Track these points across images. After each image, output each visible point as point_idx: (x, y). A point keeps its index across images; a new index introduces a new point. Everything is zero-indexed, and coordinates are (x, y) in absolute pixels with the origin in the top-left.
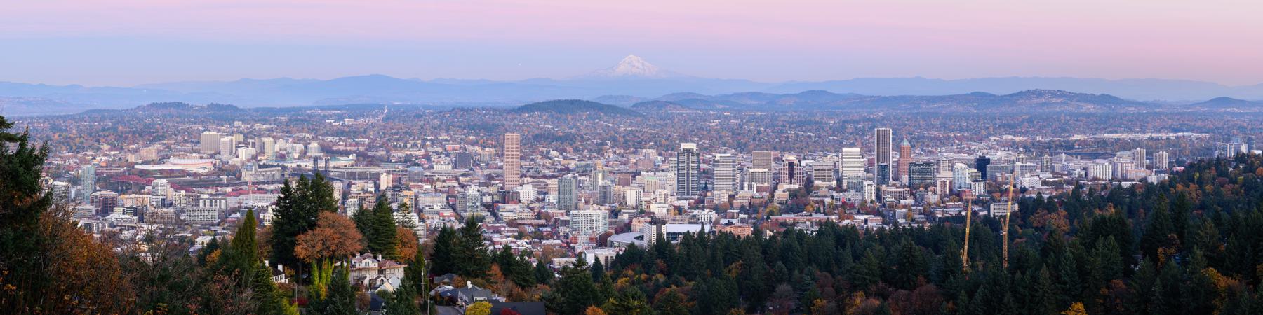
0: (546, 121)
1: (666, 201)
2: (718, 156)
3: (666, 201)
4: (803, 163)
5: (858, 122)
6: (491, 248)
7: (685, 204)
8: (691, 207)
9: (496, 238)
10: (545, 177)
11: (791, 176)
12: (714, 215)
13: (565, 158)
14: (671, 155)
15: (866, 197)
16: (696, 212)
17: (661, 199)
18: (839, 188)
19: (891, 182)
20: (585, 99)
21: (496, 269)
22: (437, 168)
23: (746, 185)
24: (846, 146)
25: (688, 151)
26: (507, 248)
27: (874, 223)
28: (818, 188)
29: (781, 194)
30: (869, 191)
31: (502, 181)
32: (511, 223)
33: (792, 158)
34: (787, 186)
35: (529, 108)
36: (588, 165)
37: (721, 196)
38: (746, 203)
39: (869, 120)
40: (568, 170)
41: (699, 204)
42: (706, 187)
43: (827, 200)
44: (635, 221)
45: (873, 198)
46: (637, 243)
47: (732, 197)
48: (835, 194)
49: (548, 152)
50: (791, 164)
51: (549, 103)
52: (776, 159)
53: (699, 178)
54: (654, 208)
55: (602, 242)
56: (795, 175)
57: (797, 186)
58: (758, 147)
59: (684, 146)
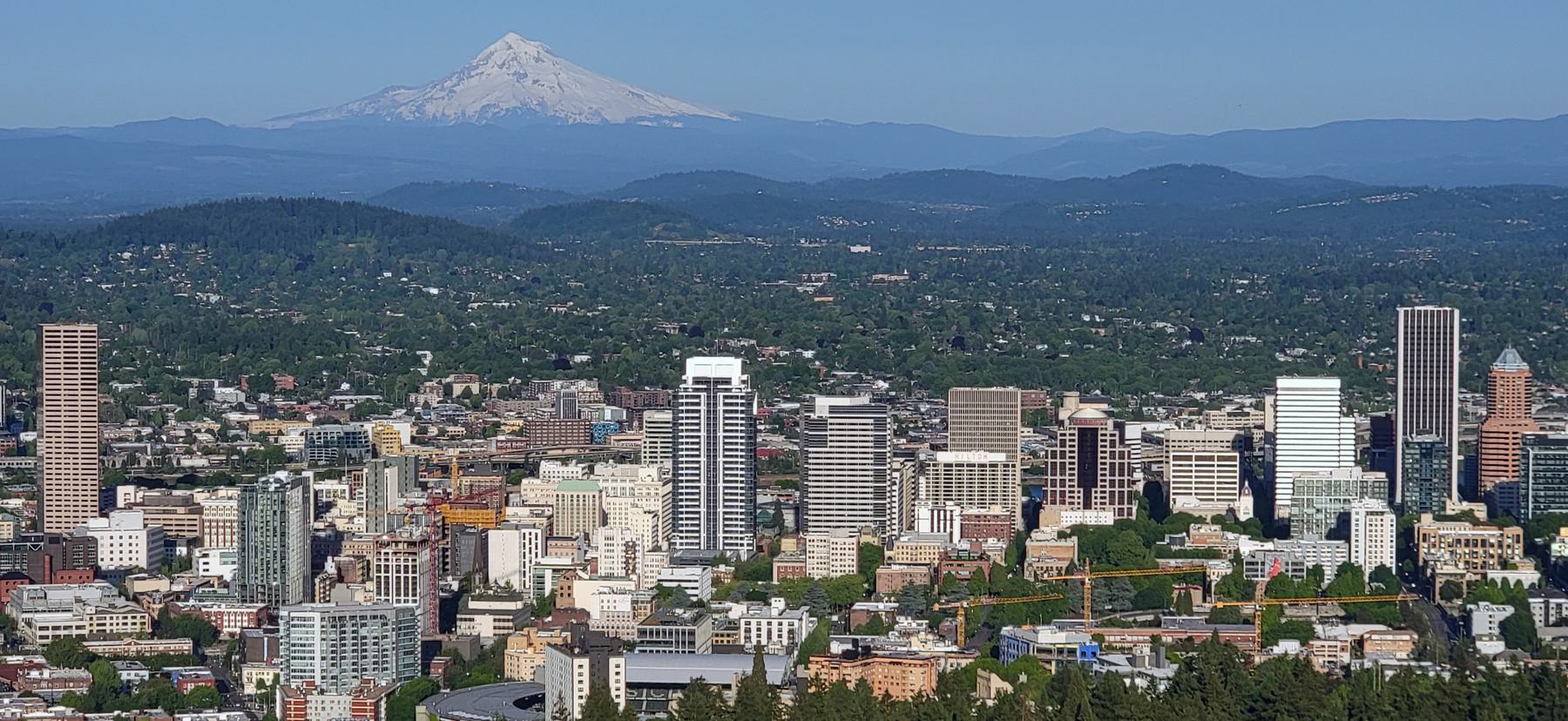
0: (200, 279)
1: (630, 566)
2: (823, 404)
3: (630, 566)
4: (1133, 431)
5: (1338, 284)
7: (697, 581)
8: (723, 593)
10: (191, 479)
11: (1088, 480)
12: (805, 625)
13: (268, 412)
14: (654, 405)
15: (1359, 558)
16: (737, 610)
17: (611, 561)
18: (1269, 525)
19: (1454, 505)
20: (341, 196)
23: (923, 513)
24: (1293, 370)
25: (711, 385)
27: (1391, 649)
28: (1186, 520)
29: (1050, 548)
30: (1375, 545)
31: (36, 496)
32: (66, 651)
33: (1091, 412)
34: (1071, 517)
35: (141, 229)
36: (352, 439)
37: (828, 553)
38: (921, 576)
39: (1379, 275)
40: (280, 458)
41: (753, 581)
42: (777, 521)
43: (1218, 570)
44: (515, 644)
45: (1389, 559)
47: (870, 558)
48: (1247, 546)
49: (206, 394)
50: (1088, 437)
51: (209, 209)
52: (1041, 420)
53: (753, 487)
54: (586, 595)
56: (1103, 475)
57: (1107, 518)
58: (973, 374)
59: (698, 367)
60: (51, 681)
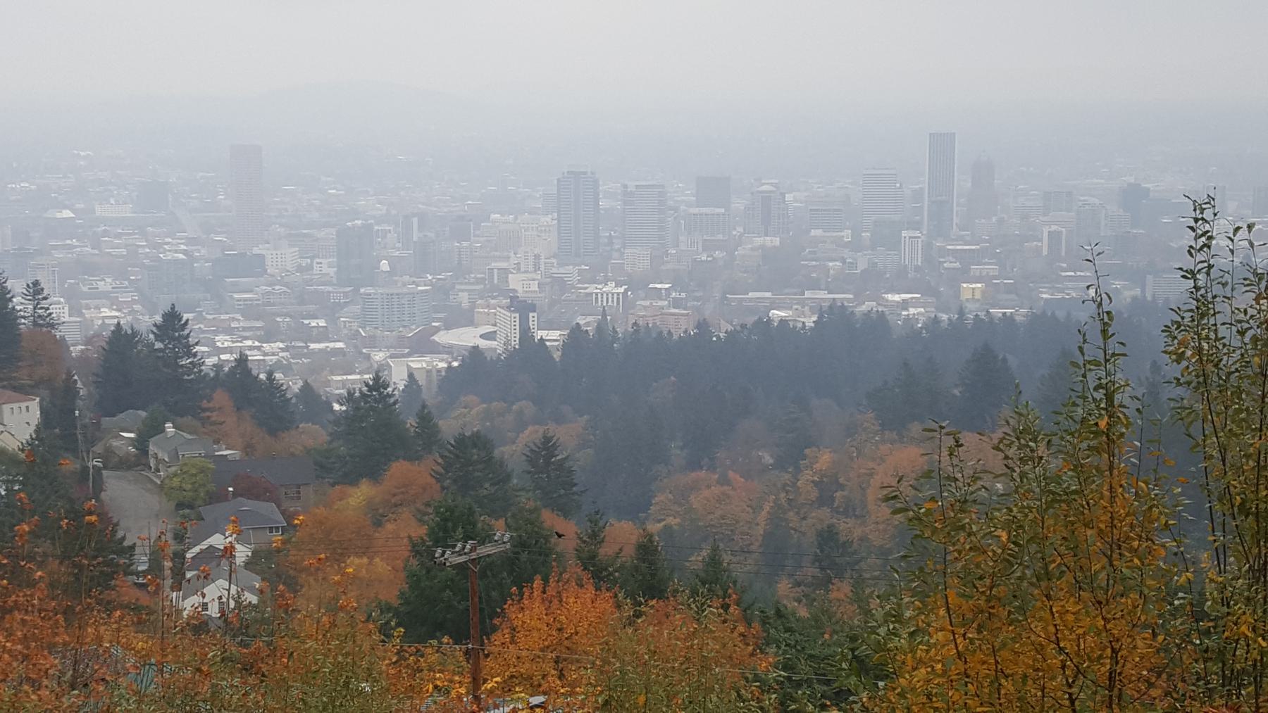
3: (536, 268)
6: (211, 361)
9: (223, 341)
21: (221, 398)
22: (99, 211)
26: (242, 361)
34: (759, 241)
46: (483, 344)
54: (516, 283)
55: (423, 345)
57: (777, 241)
60: (244, 329)
